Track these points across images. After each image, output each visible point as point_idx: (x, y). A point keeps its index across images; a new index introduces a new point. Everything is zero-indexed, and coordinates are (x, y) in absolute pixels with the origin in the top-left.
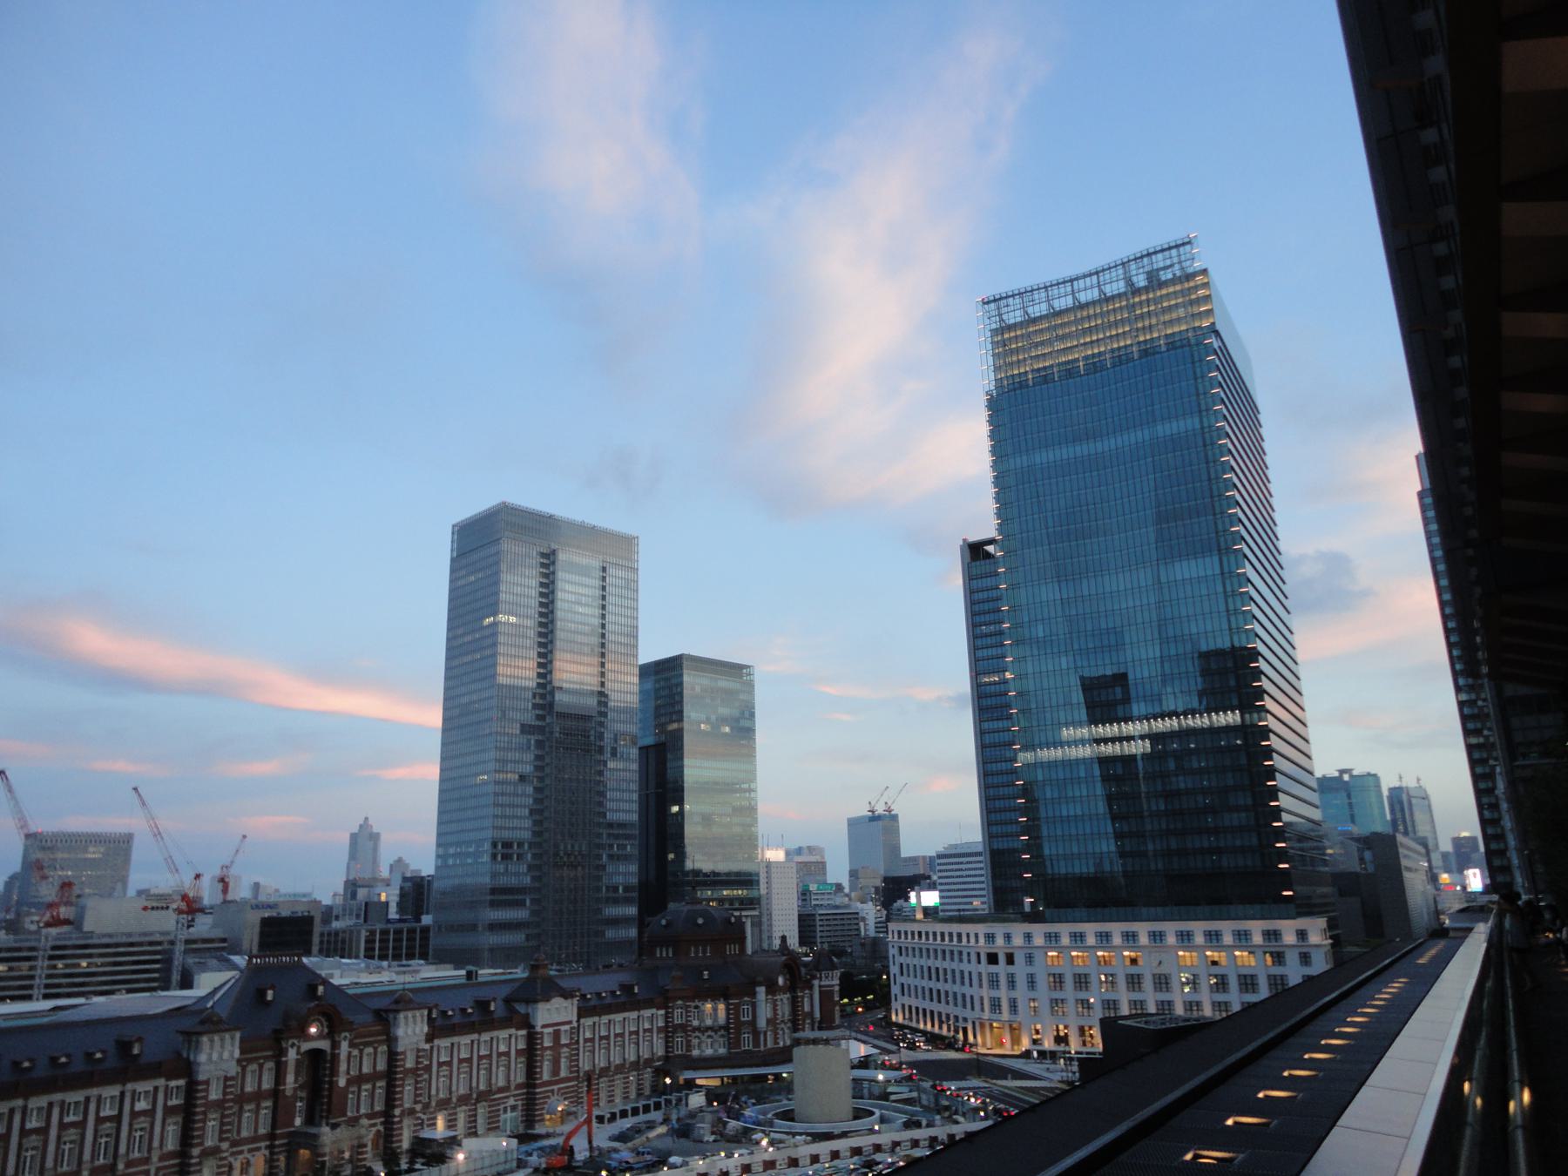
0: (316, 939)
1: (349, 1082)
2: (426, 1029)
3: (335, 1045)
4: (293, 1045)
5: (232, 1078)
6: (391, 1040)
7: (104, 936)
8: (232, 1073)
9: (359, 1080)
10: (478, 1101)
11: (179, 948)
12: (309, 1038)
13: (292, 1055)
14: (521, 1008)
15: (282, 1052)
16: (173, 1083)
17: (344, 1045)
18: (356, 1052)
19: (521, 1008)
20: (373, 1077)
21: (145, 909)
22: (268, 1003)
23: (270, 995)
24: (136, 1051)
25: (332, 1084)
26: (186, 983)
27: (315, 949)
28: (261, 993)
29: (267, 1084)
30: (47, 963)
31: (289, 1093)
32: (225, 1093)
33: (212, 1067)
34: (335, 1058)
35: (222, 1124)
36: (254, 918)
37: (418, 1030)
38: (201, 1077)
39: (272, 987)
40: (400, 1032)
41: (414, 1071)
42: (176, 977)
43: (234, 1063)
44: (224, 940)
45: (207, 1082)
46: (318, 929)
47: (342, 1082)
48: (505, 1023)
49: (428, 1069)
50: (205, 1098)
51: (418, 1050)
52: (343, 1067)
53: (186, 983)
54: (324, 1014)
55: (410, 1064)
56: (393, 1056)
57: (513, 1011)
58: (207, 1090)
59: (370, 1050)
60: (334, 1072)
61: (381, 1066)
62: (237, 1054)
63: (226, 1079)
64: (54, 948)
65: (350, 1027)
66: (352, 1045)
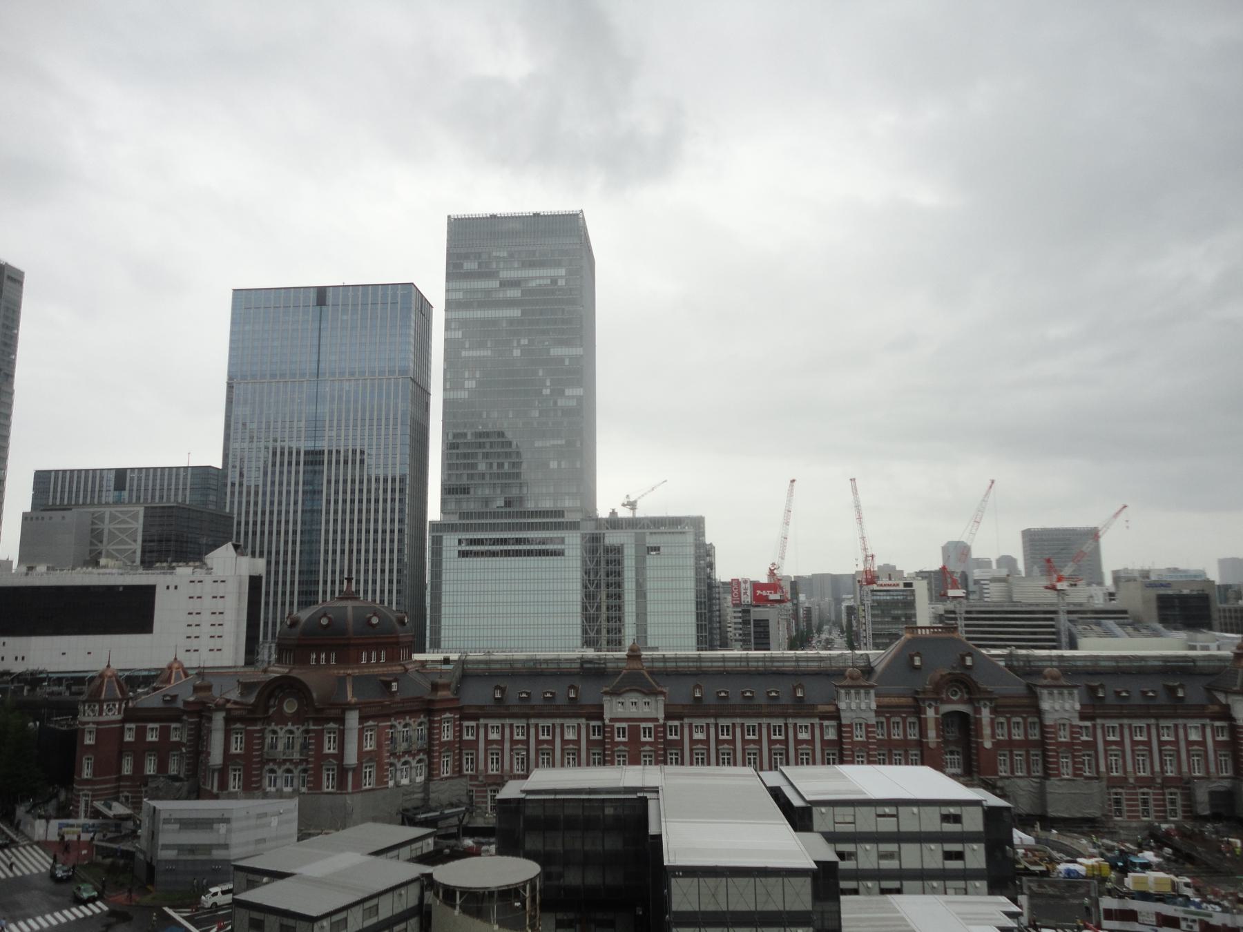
0: (1215, 615)
1: (998, 745)
2: (1078, 707)
3: (978, 711)
4: (930, 706)
5: (873, 726)
6: (1039, 713)
7: (1031, 605)
8: (873, 721)
9: (1011, 744)
10: (1163, 787)
11: (1063, 618)
12: (950, 702)
13: (930, 713)
14: (1221, 698)
15: (918, 711)
16: (826, 723)
17: (986, 714)
18: (1002, 720)
19: (1221, 698)
20: (1026, 744)
21: (1047, 588)
22: (917, 668)
23: (917, 661)
24: (799, 694)
25: (980, 746)
26: (1073, 645)
27: (1216, 623)
28: (912, 660)
29: (913, 735)
30: (964, 622)
31: (932, 745)
32: (868, 737)
33: (854, 715)
34: (978, 722)
35: (1074, 763)
36: (1152, 593)
37: (1067, 706)
38: (844, 722)
39: (918, 654)
40: (1046, 705)
41: (1069, 746)
42: (1064, 639)
43: (873, 714)
44: (1125, 612)
45: (850, 726)
46: (1217, 605)
47: (988, 744)
48: (1198, 712)
49: (1092, 745)
50: (851, 738)
51: (1072, 726)
52: (987, 731)
53: (1073, 645)
54: (962, 683)
55: (1064, 737)
56: (1043, 727)
57: (1214, 701)
58: (851, 732)
59: (1019, 720)
60: (979, 734)
61: (1035, 735)
62: (874, 706)
63: (868, 726)
64: (967, 612)
65: (990, 697)
66: (994, 711)
